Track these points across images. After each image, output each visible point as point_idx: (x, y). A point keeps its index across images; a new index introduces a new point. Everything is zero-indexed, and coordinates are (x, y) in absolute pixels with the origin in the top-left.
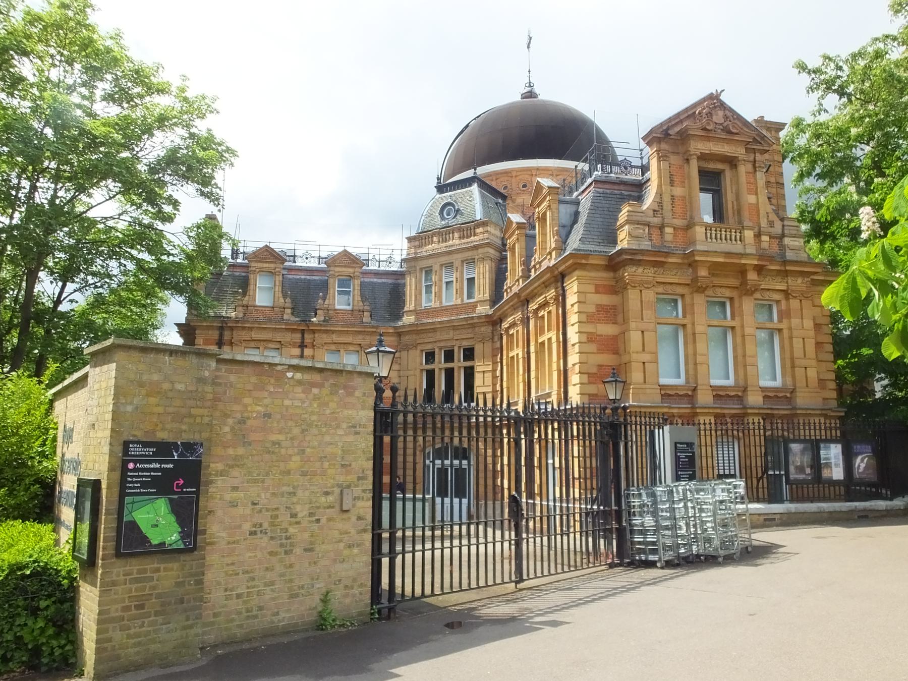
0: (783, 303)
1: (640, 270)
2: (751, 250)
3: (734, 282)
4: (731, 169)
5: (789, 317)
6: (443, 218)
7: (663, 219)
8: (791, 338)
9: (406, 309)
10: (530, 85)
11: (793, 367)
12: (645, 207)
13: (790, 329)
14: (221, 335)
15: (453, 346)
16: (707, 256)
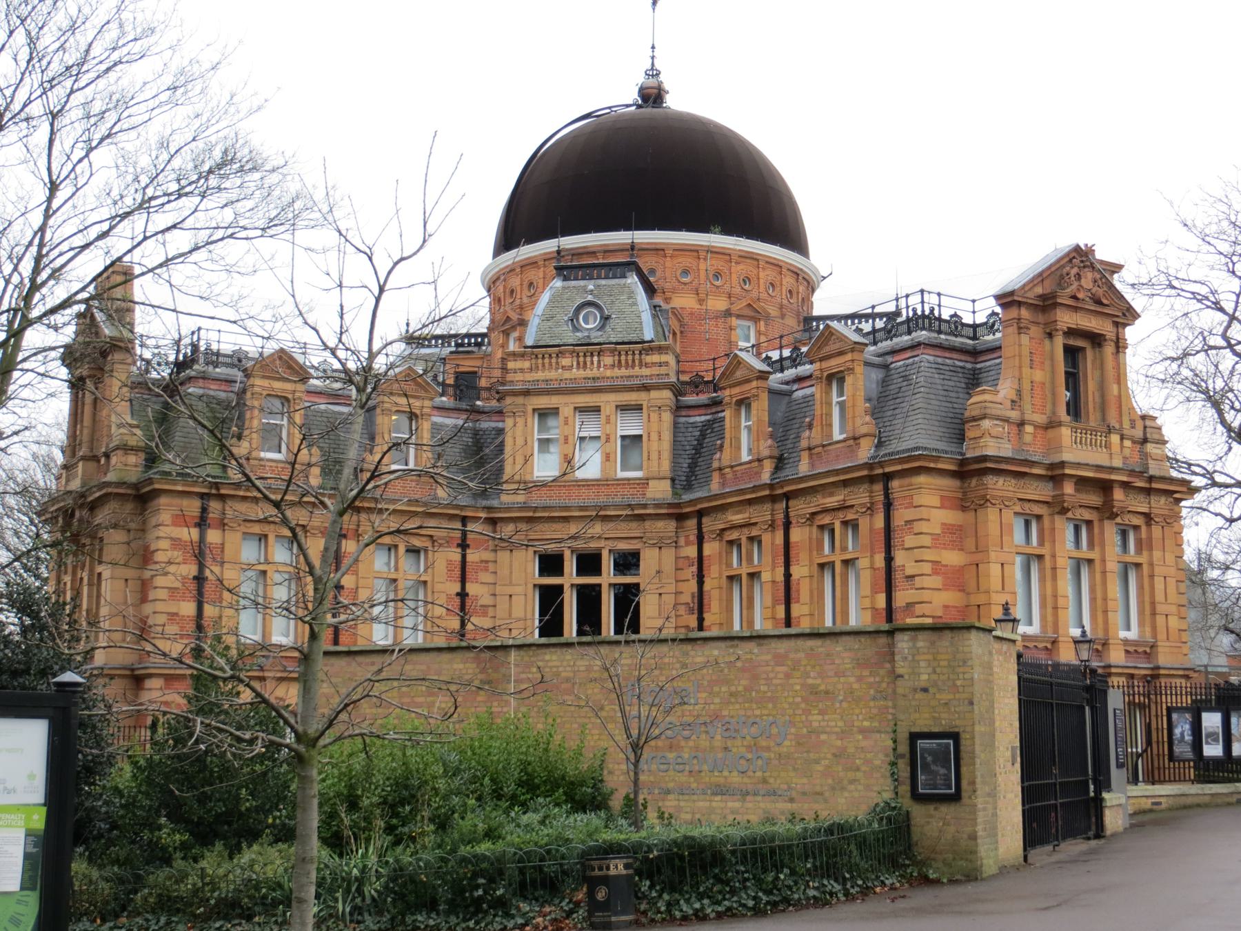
0: (1144, 528)
1: (1001, 481)
2: (1117, 462)
3: (1095, 499)
4: (1093, 347)
5: (1151, 549)
6: (576, 329)
7: (1023, 414)
8: (1152, 576)
9: (505, 478)
10: (653, 73)
11: (1154, 614)
12: (1002, 394)
13: (1151, 565)
14: (204, 510)
15: (600, 549)
16: (1077, 469)
